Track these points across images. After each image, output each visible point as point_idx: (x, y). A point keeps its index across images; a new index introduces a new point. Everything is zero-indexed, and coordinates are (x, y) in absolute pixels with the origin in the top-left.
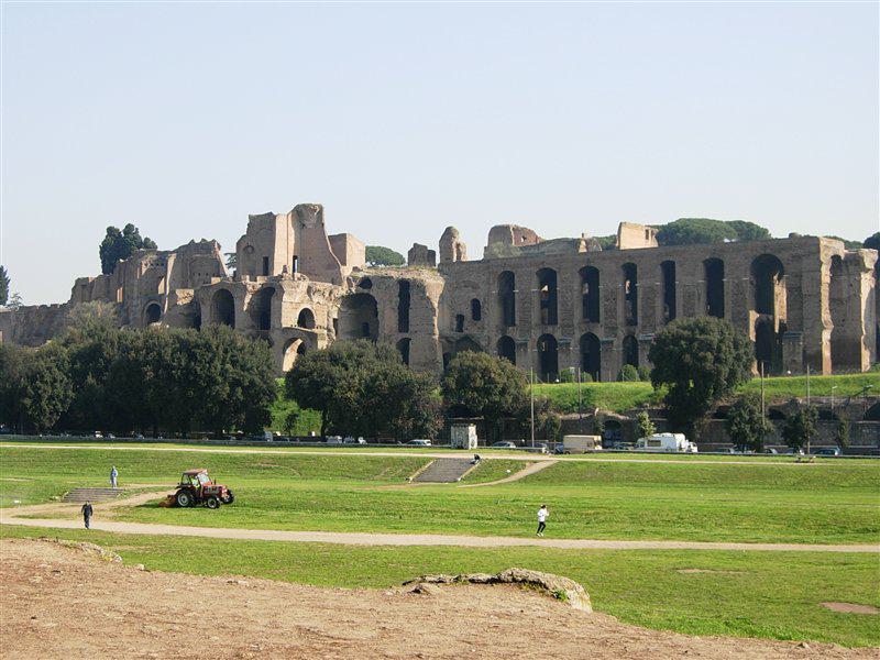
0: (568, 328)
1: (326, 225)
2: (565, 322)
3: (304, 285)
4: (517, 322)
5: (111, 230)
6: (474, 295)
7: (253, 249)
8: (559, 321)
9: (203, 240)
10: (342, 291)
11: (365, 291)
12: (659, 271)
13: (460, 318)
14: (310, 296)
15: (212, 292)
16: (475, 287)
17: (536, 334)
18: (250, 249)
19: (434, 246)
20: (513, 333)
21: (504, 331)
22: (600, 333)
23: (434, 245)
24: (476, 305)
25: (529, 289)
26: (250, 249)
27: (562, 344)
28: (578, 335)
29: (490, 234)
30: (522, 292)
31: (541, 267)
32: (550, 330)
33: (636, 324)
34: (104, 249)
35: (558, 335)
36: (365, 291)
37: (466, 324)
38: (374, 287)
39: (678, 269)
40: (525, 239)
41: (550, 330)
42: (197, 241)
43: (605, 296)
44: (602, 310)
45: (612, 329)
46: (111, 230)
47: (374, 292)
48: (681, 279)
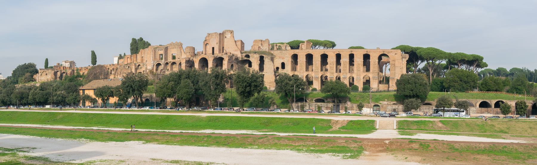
2: (316, 71)
5: (134, 40)
6: (282, 61)
16: (283, 58)
24: (283, 66)
36: (248, 59)
46: (134, 40)
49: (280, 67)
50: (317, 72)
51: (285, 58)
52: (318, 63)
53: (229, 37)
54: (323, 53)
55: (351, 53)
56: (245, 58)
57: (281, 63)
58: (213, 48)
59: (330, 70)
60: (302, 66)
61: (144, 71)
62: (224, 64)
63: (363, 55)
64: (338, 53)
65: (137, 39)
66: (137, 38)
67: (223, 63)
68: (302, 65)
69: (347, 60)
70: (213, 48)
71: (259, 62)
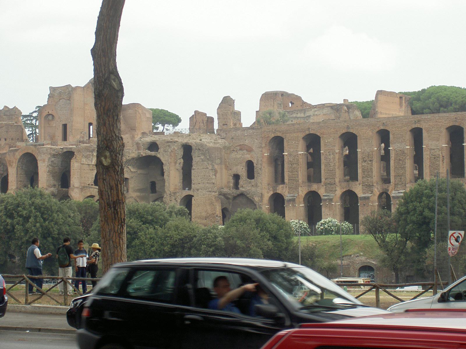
0: (330, 186)
2: (328, 181)
4: (286, 180)
6: (248, 157)
7: (53, 116)
8: (323, 180)
9: (6, 107)
12: (409, 136)
13: (237, 177)
16: (250, 150)
17: (302, 192)
19: (212, 112)
20: (281, 189)
21: (274, 188)
22: (359, 190)
23: (212, 112)
24: (250, 166)
26: (50, 117)
27: (326, 200)
28: (339, 192)
29: (261, 100)
30: (290, 155)
31: (307, 133)
32: (314, 187)
33: (390, 182)
35: (322, 192)
36: (153, 153)
37: (241, 182)
38: (161, 150)
39: (425, 134)
40: (292, 103)
41: (314, 187)
43: (363, 158)
44: (360, 171)
45: (369, 187)
47: (161, 155)
48: (427, 143)
50: (331, 184)
52: (334, 158)
54: (344, 131)
56: (149, 153)
57: (244, 164)
58: (65, 126)
59: (363, 177)
60: (294, 168)
64: (382, 128)
68: (295, 165)
69: (408, 147)
70: (65, 126)
71: (182, 161)
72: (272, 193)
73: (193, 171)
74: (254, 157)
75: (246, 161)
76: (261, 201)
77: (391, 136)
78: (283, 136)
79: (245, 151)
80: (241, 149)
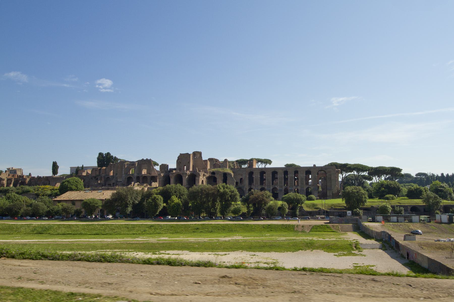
1: (202, 157)
3: (203, 173)
5: (100, 154)
6: (241, 177)
7: (181, 162)
10: (208, 175)
11: (214, 175)
14: (203, 177)
15: (175, 175)
16: (242, 175)
18: (180, 163)
25: (291, 175)
26: (180, 163)
34: (98, 159)
36: (214, 175)
38: (216, 174)
42: (145, 159)
43: (279, 178)
46: (100, 154)
49: (239, 181)
51: (243, 175)
53: (198, 158)
55: (296, 170)
59: (279, 184)
61: (114, 183)
62: (197, 180)
63: (305, 172)
64: (286, 170)
65: (104, 154)
66: (104, 152)
67: (196, 179)
72: (249, 188)
73: (227, 181)
74: (243, 177)
75: (240, 178)
76: (246, 190)
77: (288, 172)
78: (253, 171)
79: (240, 175)
80: (239, 175)
